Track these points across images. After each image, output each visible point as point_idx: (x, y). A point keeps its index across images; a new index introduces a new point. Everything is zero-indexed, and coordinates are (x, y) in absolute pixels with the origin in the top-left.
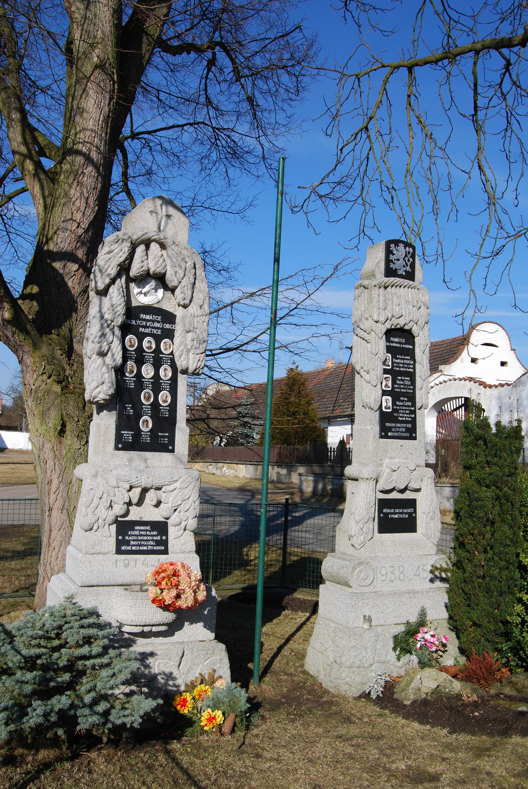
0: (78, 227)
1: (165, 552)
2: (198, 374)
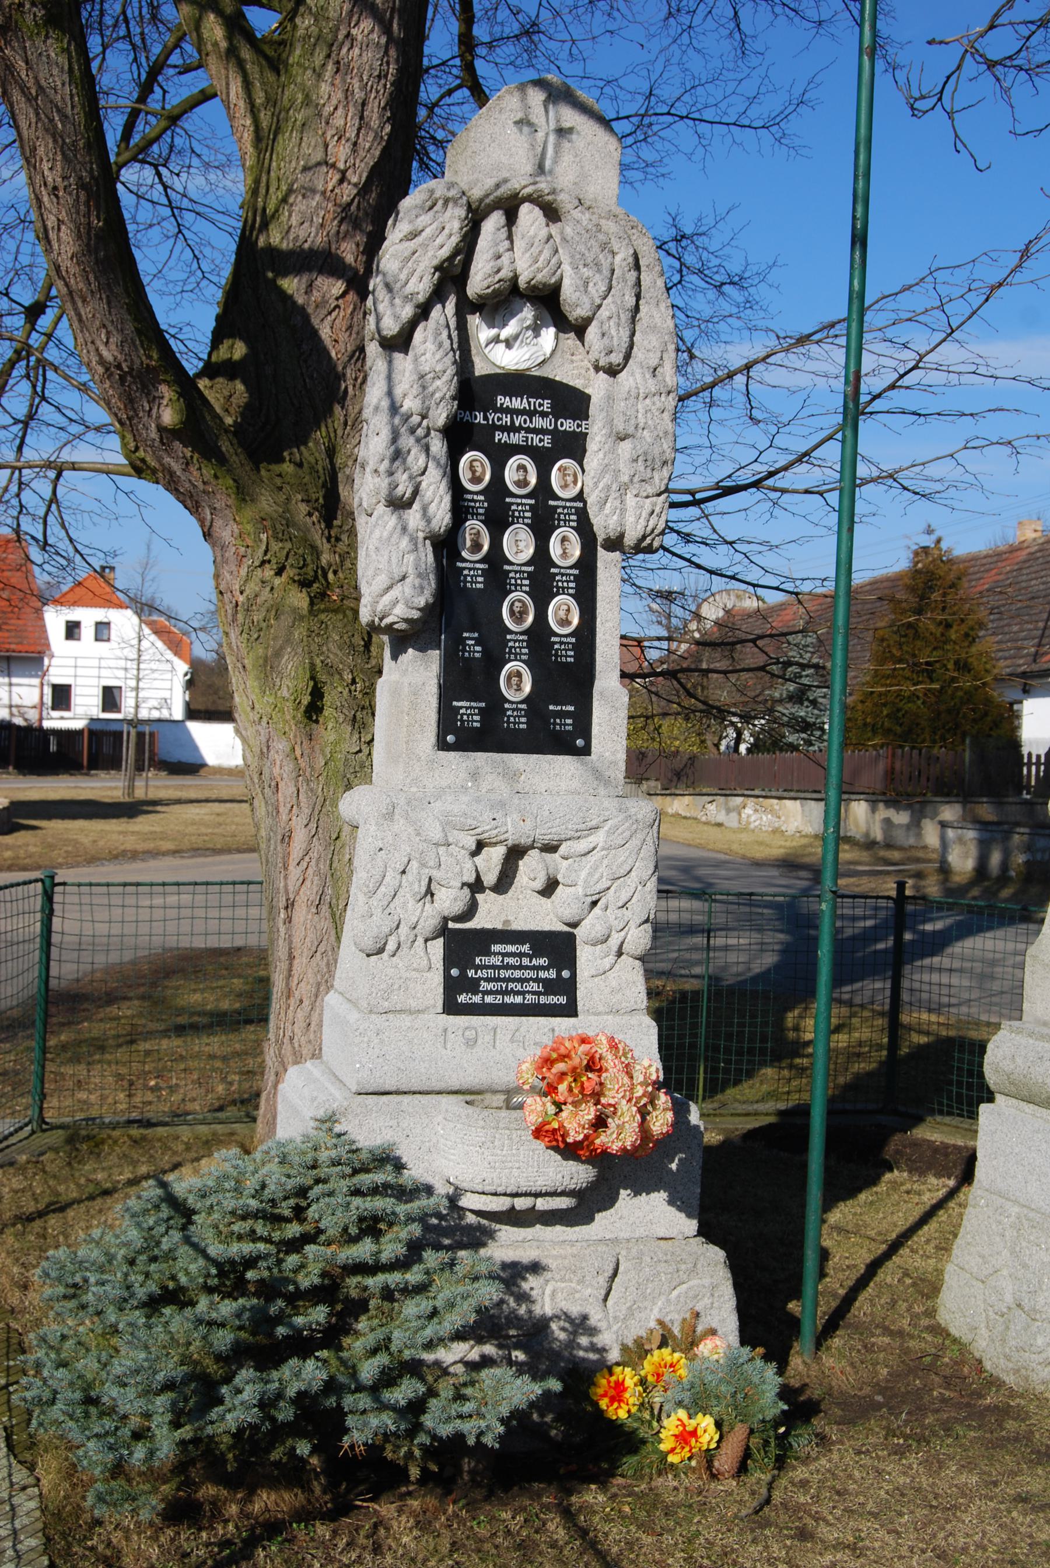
0: (341, 181)
1: (570, 1010)
2: (650, 550)
